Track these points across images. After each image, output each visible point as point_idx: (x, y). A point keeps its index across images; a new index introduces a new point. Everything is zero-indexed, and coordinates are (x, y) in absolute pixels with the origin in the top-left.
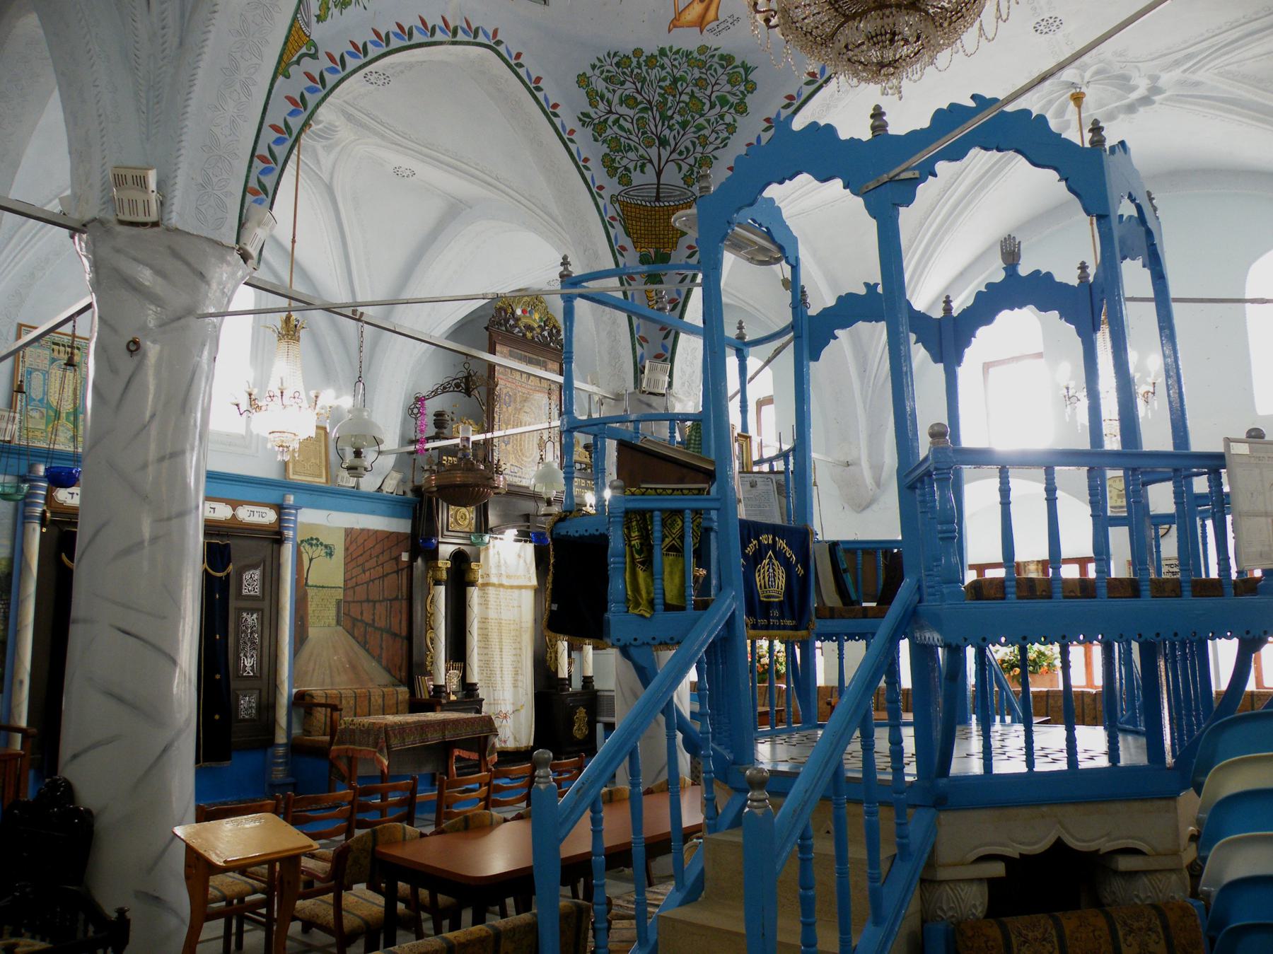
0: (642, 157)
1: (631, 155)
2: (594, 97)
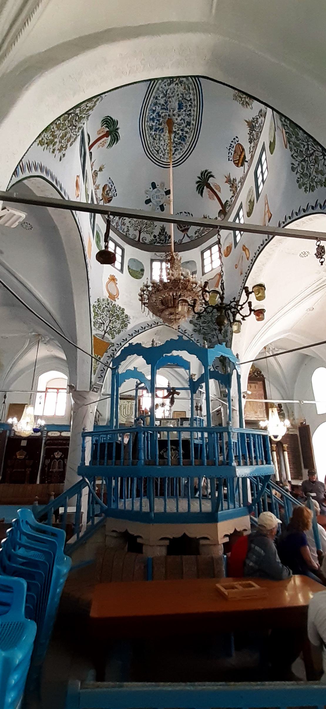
0: (212, 335)
1: (210, 335)
2: (195, 325)
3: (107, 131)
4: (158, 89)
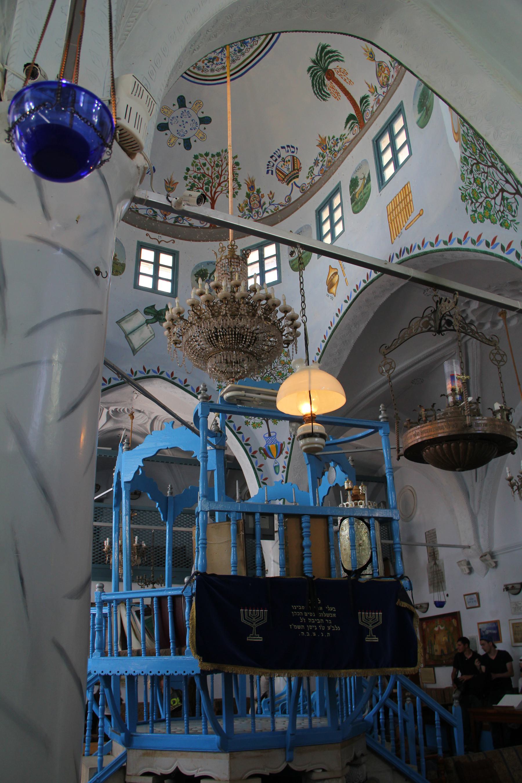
3: (329, 79)
4: (233, 61)
